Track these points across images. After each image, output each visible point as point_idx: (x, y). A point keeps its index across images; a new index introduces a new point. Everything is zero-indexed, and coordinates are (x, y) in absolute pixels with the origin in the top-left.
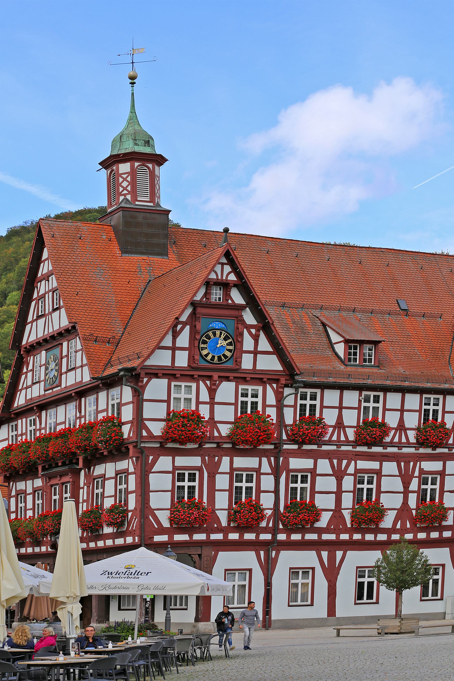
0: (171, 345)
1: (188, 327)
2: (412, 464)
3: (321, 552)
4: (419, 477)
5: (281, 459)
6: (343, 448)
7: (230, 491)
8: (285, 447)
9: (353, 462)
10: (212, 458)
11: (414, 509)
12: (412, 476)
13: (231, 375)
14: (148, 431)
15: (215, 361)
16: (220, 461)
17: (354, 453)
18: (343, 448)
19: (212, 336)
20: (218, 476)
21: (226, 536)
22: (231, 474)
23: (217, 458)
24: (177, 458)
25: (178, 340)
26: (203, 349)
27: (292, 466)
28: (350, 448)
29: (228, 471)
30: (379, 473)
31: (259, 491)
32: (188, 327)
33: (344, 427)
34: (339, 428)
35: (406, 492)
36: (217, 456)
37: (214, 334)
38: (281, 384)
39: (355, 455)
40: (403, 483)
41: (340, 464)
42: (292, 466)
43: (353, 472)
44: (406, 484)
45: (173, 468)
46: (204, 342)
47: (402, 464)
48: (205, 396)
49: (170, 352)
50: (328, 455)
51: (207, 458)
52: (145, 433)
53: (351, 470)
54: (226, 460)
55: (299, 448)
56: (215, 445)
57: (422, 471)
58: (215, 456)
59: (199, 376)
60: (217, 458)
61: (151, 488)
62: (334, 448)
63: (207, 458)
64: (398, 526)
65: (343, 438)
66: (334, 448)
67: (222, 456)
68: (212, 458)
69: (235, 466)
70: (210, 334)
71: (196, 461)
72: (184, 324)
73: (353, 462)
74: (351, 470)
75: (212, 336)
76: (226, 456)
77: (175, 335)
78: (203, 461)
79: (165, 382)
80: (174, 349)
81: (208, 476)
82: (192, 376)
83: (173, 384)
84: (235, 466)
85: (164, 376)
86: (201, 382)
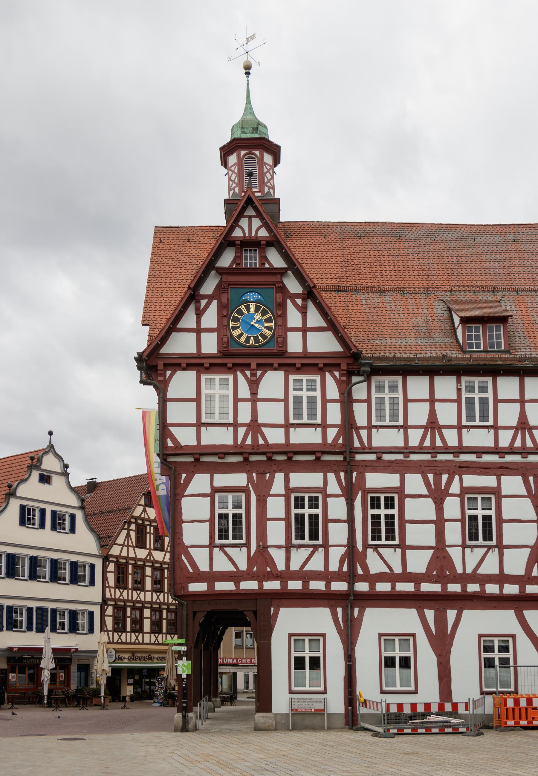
0: (194, 326)
1: (215, 303)
5: (355, 474)
6: (441, 457)
8: (358, 457)
10: (261, 475)
13: (276, 361)
14: (174, 440)
15: (251, 343)
16: (272, 478)
17: (458, 465)
18: (441, 457)
19: (245, 312)
20: (269, 499)
23: (268, 475)
24: (216, 476)
25: (203, 319)
26: (235, 328)
28: (450, 457)
29: (283, 492)
32: (215, 303)
33: (440, 428)
34: (433, 429)
36: (269, 472)
37: (248, 308)
38: (343, 370)
39: (460, 467)
45: (211, 490)
46: (236, 320)
48: (244, 391)
49: (194, 335)
51: (254, 475)
52: (170, 443)
54: (279, 477)
55: (379, 458)
56: (263, 458)
58: (265, 473)
59: (234, 365)
60: (268, 475)
62: (427, 457)
63: (254, 475)
66: (427, 457)
67: (275, 472)
68: (261, 475)
69: (292, 485)
70: (243, 308)
72: (210, 298)
75: (245, 312)
76: (280, 471)
77: (199, 314)
78: (250, 479)
79: (192, 375)
80: (199, 331)
81: (258, 500)
82: (225, 365)
83: (204, 377)
84: (292, 485)
85: (189, 367)
86: (239, 374)
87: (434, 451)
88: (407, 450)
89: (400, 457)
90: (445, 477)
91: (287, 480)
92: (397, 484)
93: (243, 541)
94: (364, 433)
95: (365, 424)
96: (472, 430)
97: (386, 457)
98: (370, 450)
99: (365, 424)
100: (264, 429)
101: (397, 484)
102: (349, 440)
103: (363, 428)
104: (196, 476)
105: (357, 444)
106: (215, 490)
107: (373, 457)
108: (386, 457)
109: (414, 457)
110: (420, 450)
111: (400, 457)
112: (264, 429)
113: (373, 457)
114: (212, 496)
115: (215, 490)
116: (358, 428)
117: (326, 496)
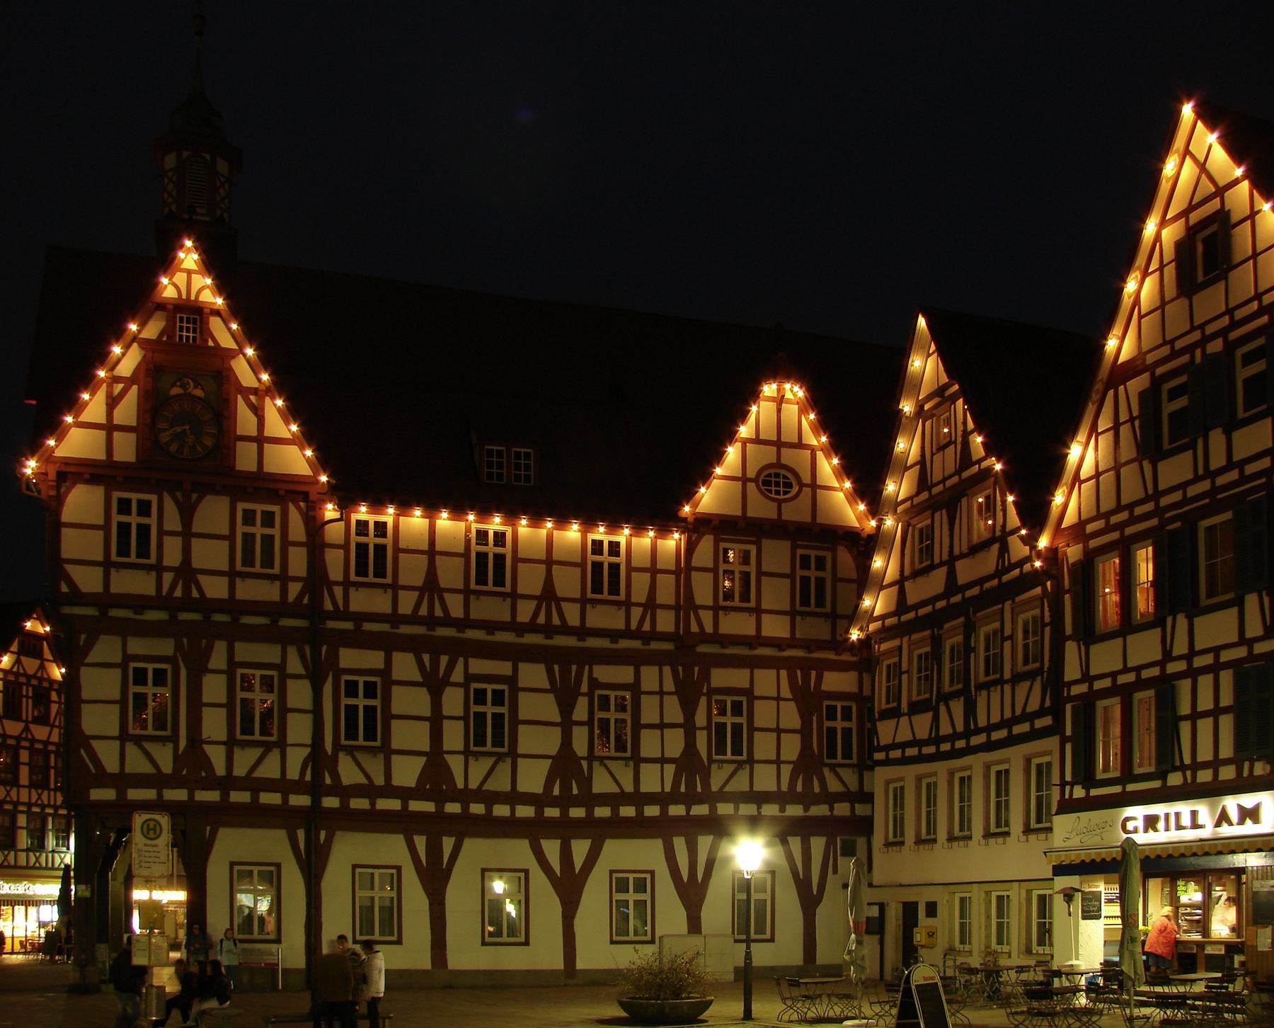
2: (574, 668)
3: (414, 837)
4: (590, 695)
5: (324, 648)
7: (230, 705)
8: (332, 624)
9: (461, 660)
11: (583, 758)
12: (576, 693)
21: (225, 796)
22: (230, 673)
27: (343, 664)
29: (224, 666)
30: (512, 680)
31: (285, 710)
33: (441, 591)
35: (567, 725)
40: (560, 704)
41: (435, 663)
42: (343, 664)
43: (461, 680)
44: (566, 707)
47: (556, 667)
50: (413, 645)
51: (185, 640)
53: (458, 676)
54: (220, 647)
57: (593, 683)
61: (85, 695)
62: (420, 630)
63: (185, 640)
64: (556, 792)
65: (438, 612)
66: (420, 630)
71: (166, 647)
73: (461, 660)
74: (458, 676)
76: (221, 637)
78: (178, 647)
87: (431, 622)
88: (394, 618)
89: (385, 627)
90: (444, 660)
91: (231, 652)
92: (381, 666)
93: (168, 733)
94: (338, 591)
95: (341, 579)
96: (483, 598)
97: (367, 626)
98: (345, 615)
99: (341, 579)
100: (201, 578)
101: (381, 666)
102: (317, 600)
103: (338, 583)
104: (102, 637)
105: (328, 606)
106: (127, 658)
107: (348, 625)
108: (367, 626)
109: (405, 629)
110: (413, 619)
111: (385, 627)
112: (201, 578)
113: (348, 625)
114: (123, 666)
115: (127, 658)
116: (331, 584)
117: (284, 676)
